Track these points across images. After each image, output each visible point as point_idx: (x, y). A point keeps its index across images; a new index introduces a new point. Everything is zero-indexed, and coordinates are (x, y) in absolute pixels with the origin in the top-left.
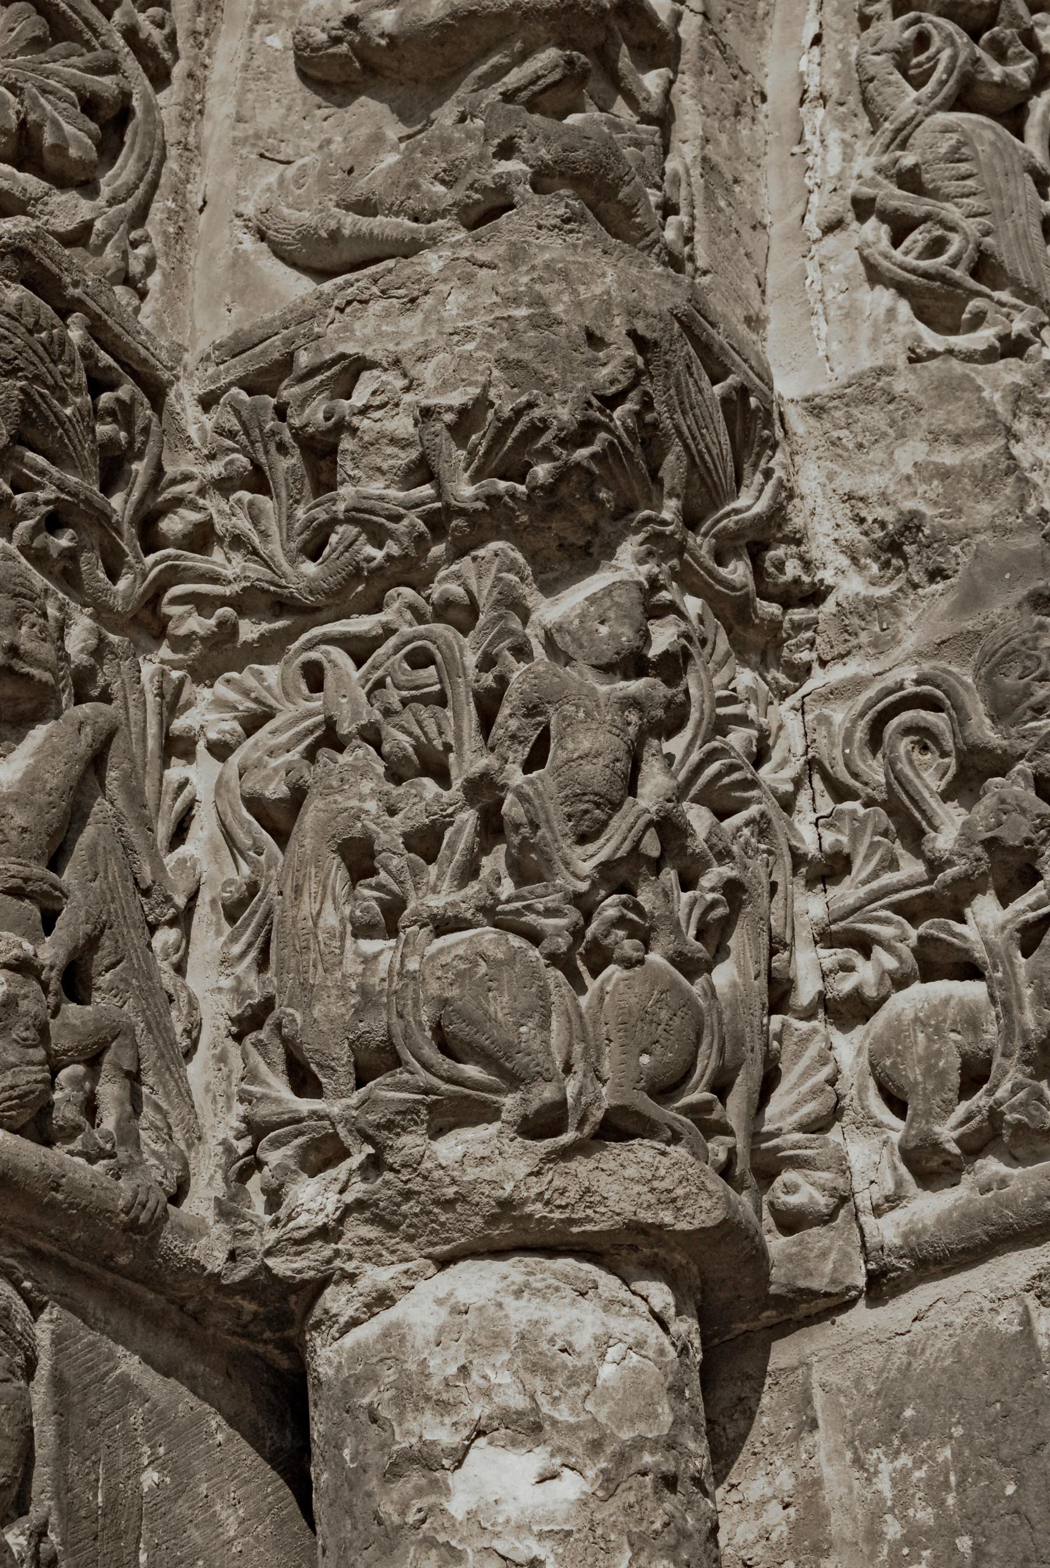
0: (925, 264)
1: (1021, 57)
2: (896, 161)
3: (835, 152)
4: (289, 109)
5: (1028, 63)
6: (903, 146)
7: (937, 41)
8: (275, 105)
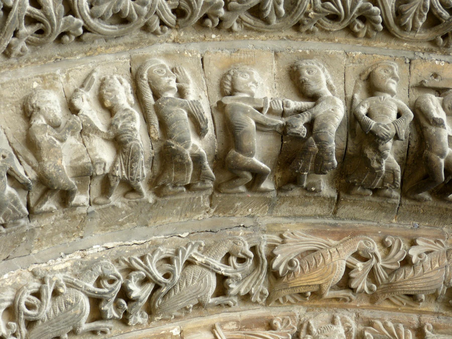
0: (23, 305)
1: (119, 314)
2: (61, 286)
3: (62, 266)
4: (13, 98)
5: (116, 315)
6: (68, 286)
7: (112, 286)
8: (12, 93)
